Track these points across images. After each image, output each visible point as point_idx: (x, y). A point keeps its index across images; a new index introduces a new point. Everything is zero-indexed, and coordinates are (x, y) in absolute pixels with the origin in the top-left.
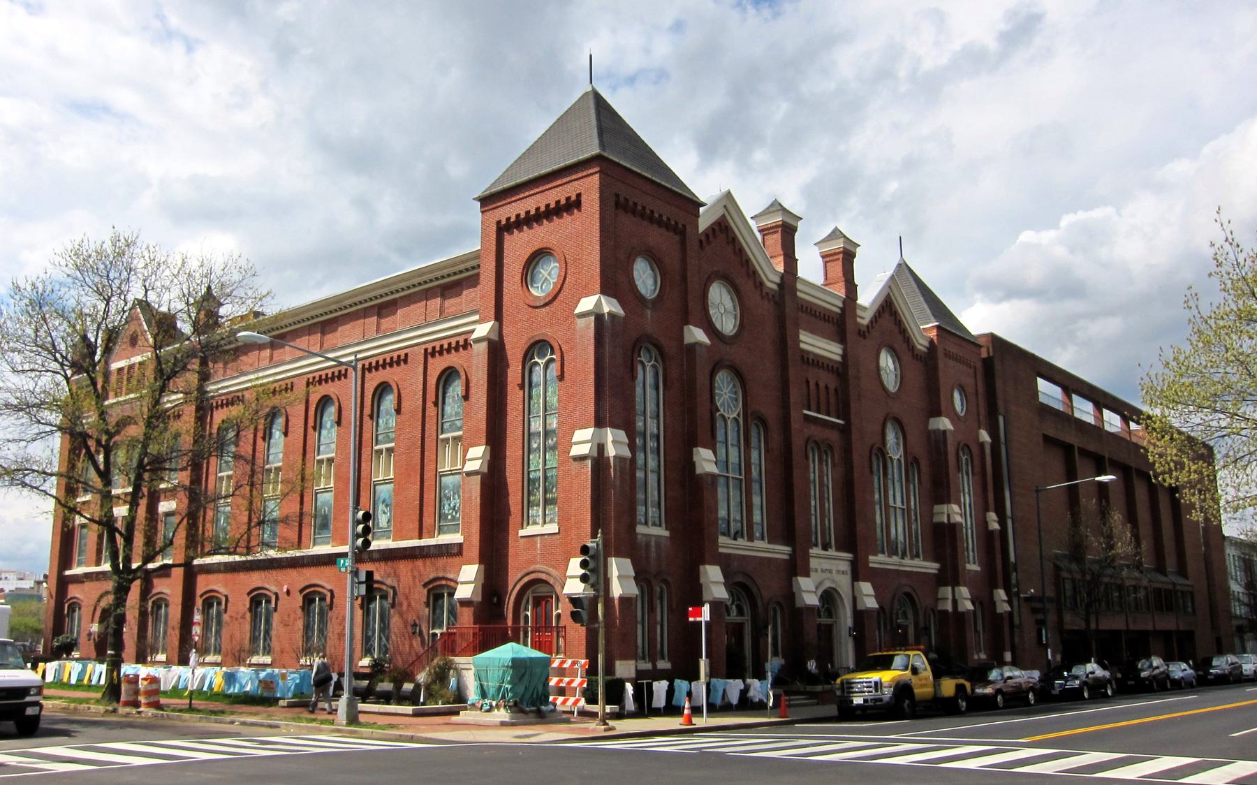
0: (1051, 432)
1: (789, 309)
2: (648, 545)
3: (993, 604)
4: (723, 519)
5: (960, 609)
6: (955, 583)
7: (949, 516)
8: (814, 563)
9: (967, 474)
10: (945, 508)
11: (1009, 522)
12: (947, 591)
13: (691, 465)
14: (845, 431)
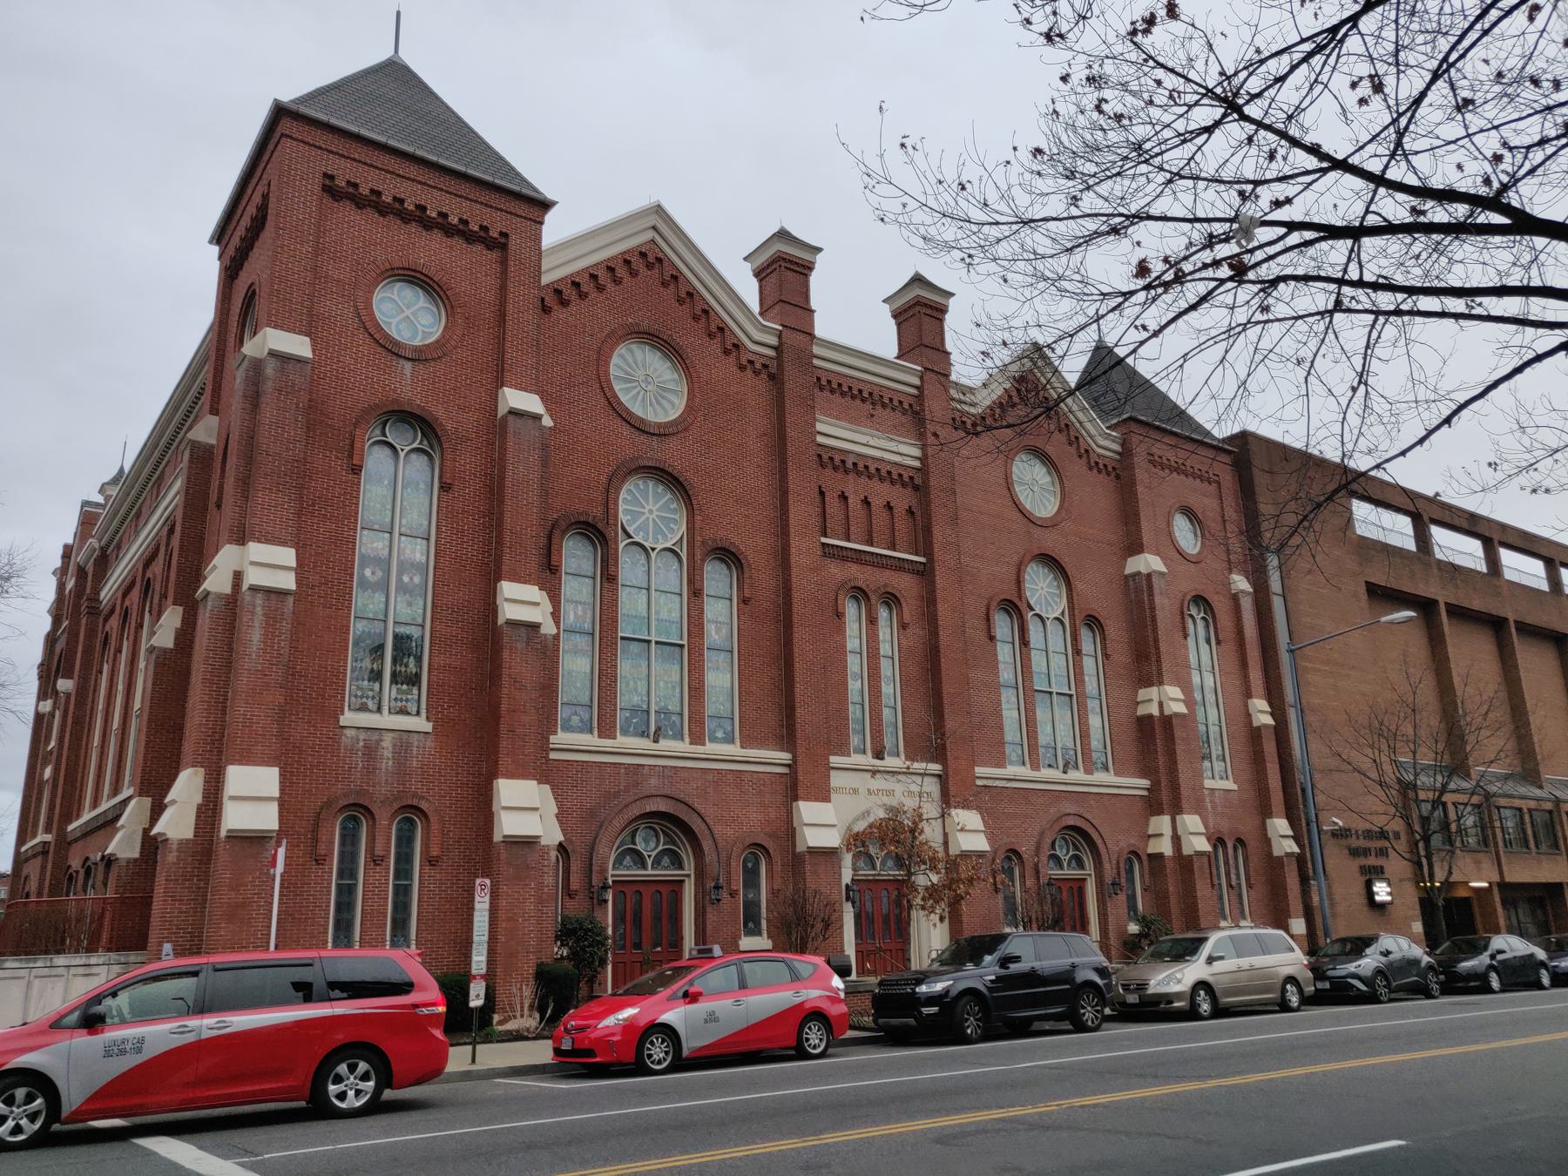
0: (1380, 579)
1: (794, 381)
2: (371, 751)
3: (1267, 842)
5: (1186, 851)
6: (1176, 809)
7: (1161, 705)
8: (836, 779)
9: (1208, 641)
10: (1153, 692)
11: (1292, 715)
12: (1162, 823)
14: (925, 573)
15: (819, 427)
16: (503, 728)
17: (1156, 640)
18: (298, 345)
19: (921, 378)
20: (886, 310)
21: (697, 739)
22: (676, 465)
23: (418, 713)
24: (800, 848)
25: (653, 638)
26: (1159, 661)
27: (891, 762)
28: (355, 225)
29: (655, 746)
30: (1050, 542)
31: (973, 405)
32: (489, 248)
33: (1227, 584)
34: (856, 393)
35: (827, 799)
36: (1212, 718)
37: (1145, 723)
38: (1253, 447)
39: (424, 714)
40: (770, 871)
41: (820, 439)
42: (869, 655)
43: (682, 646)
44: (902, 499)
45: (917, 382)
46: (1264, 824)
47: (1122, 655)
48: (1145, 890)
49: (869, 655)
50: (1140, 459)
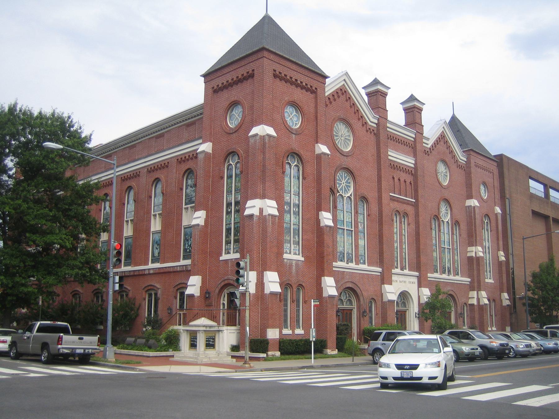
0: (537, 209)
1: (383, 137)
2: (291, 265)
3: (501, 301)
4: (341, 253)
5: (481, 303)
6: (479, 289)
7: (476, 253)
8: (394, 278)
9: (487, 230)
10: (473, 248)
11: (511, 257)
12: (474, 294)
13: (318, 221)
14: (416, 205)
15: (389, 153)
16: (325, 260)
17: (476, 230)
18: (270, 131)
19: (415, 135)
20: (401, 107)
21: (357, 263)
22: (351, 167)
23: (299, 254)
24: (385, 300)
25: (345, 228)
26: (476, 237)
27: (406, 271)
28: (281, 86)
29: (347, 265)
30: (447, 195)
31: (427, 144)
32: (311, 93)
33: (494, 210)
34: (398, 142)
35: (391, 284)
36: (488, 258)
37: (470, 259)
38: (505, 161)
39: (301, 254)
40: (376, 307)
41: (390, 158)
42: (400, 233)
43: (352, 231)
44: (409, 179)
45: (414, 136)
46: (500, 294)
47: (465, 235)
48: (467, 316)
49: (400, 233)
50: (473, 165)
